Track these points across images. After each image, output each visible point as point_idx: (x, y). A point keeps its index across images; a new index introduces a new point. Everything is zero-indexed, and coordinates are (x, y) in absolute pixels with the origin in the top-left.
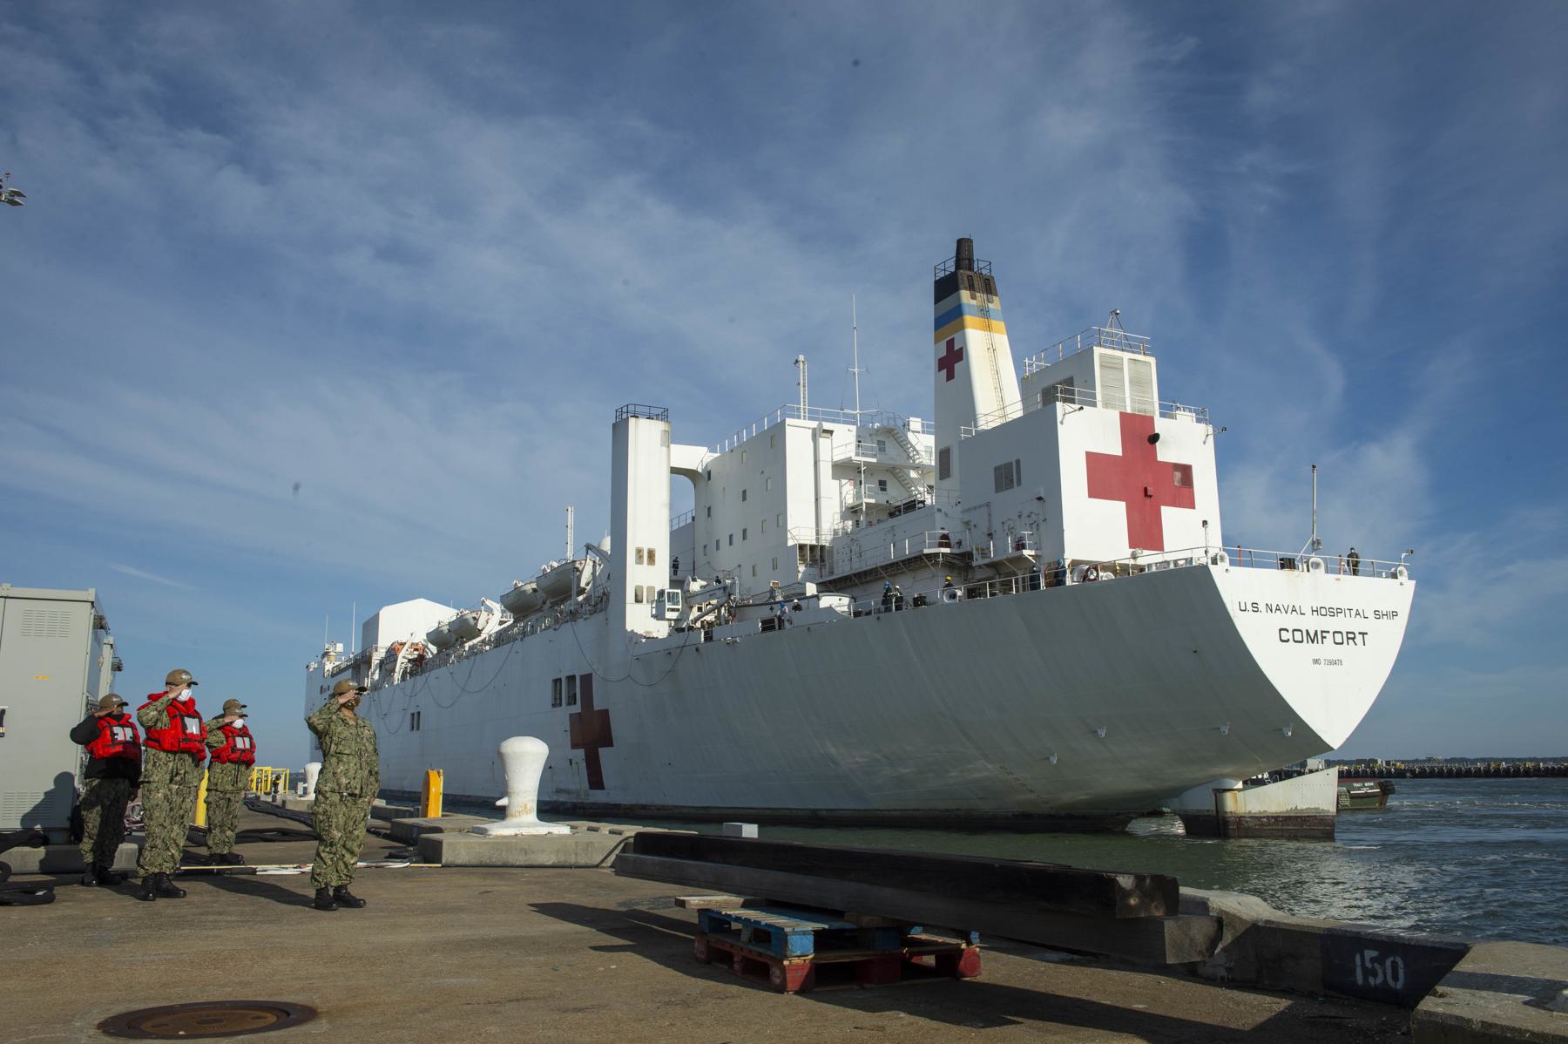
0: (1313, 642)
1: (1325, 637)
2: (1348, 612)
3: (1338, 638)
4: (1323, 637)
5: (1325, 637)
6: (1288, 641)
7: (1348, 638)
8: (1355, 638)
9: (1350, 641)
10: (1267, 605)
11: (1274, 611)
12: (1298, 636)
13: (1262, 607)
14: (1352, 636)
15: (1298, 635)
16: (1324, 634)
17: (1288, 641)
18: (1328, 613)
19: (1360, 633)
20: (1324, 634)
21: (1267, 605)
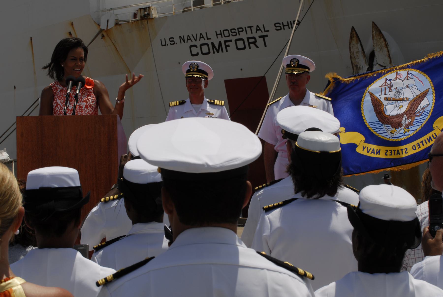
0: (218, 51)
1: (228, 46)
3: (240, 44)
4: (227, 46)
5: (228, 46)
6: (197, 54)
7: (249, 43)
8: (256, 41)
9: (252, 46)
10: (180, 37)
11: (186, 40)
13: (177, 40)
14: (253, 40)
16: (227, 44)
18: (231, 34)
19: (260, 37)
20: (227, 44)
21: (180, 37)
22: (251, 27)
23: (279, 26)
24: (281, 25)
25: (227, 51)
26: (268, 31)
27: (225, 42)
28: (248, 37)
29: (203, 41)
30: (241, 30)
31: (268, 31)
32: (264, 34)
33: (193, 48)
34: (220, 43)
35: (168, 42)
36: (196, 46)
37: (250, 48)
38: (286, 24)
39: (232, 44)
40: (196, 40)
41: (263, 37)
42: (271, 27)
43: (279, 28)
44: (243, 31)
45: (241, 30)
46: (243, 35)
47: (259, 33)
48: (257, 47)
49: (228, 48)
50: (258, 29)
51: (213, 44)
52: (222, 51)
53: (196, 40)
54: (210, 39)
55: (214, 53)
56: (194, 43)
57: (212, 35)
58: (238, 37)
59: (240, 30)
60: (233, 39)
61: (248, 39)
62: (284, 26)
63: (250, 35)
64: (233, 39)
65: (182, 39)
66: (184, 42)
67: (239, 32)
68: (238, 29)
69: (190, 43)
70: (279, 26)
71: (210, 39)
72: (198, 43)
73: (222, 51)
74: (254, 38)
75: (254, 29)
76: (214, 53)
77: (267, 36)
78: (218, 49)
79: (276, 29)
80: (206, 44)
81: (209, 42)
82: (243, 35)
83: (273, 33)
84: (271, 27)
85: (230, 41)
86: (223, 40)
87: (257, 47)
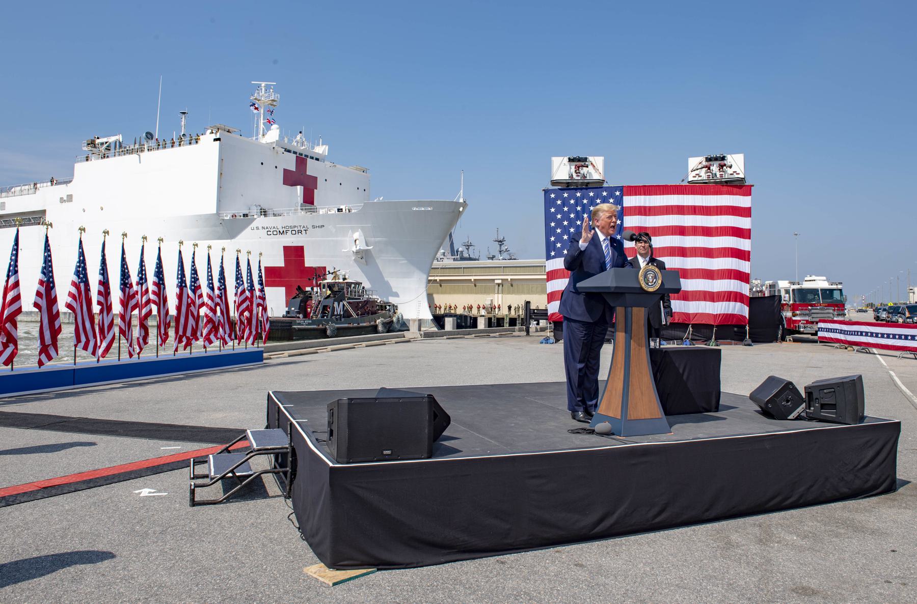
3: (294, 232)
12: (275, 233)
13: (260, 228)
23: (314, 227)
29: (274, 230)
32: (306, 229)
34: (283, 231)
35: (255, 228)
42: (310, 227)
47: (304, 229)
50: (304, 227)
51: (279, 231)
58: (293, 229)
59: (295, 227)
65: (263, 228)
69: (267, 230)
70: (314, 227)
72: (272, 230)
75: (302, 227)
81: (278, 231)
82: (296, 229)
84: (310, 227)
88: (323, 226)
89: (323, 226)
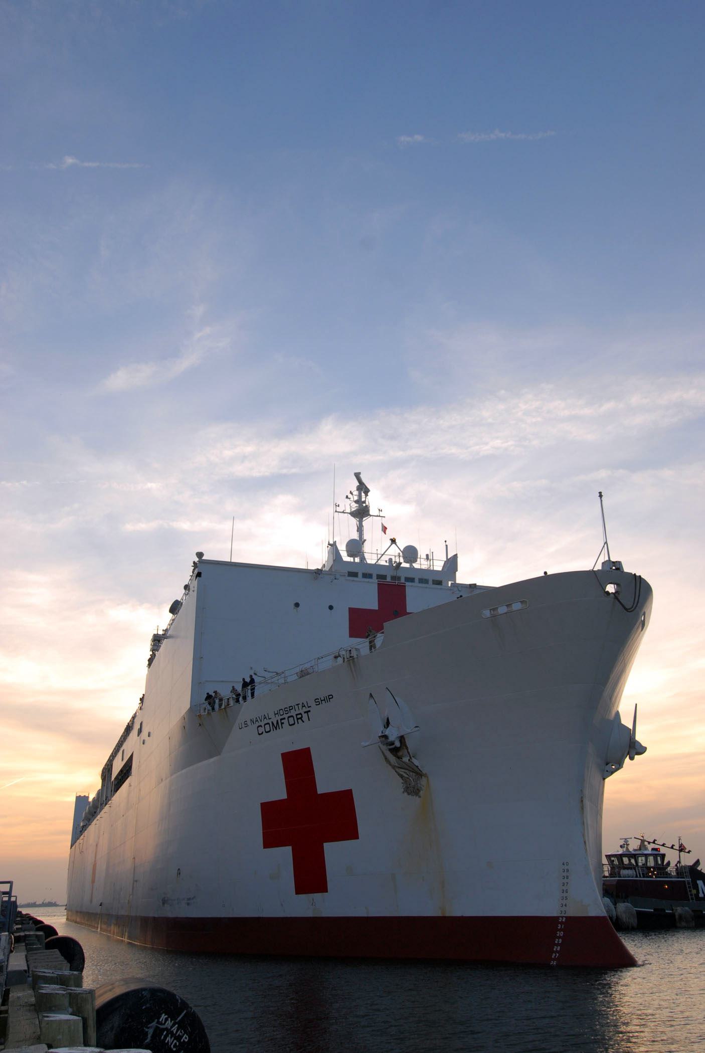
0: (276, 729)
1: (283, 723)
2: (296, 707)
3: (291, 720)
5: (283, 723)
6: (262, 733)
7: (298, 719)
8: (302, 717)
9: (300, 720)
13: (249, 723)
14: (299, 716)
15: (267, 726)
17: (262, 733)
19: (305, 712)
20: (282, 721)
22: (298, 705)
23: (318, 702)
24: (320, 701)
25: (282, 728)
26: (310, 707)
27: (281, 720)
28: (297, 713)
29: (266, 721)
30: (291, 708)
31: (310, 707)
32: (308, 709)
33: (259, 728)
35: (243, 726)
36: (261, 726)
37: (298, 723)
38: (323, 699)
39: (285, 721)
40: (261, 721)
41: (307, 712)
42: (312, 703)
43: (318, 703)
44: (292, 709)
45: (291, 708)
46: (293, 713)
48: (303, 722)
49: (283, 725)
52: (279, 728)
53: (261, 721)
54: (270, 719)
55: (273, 730)
56: (260, 724)
57: (272, 715)
59: (291, 708)
60: (286, 716)
61: (297, 715)
62: (321, 701)
63: (298, 712)
64: (286, 716)
66: (253, 722)
67: (290, 710)
68: (289, 707)
70: (318, 702)
71: (270, 719)
72: (262, 724)
73: (279, 728)
74: (300, 714)
75: (300, 706)
76: (273, 730)
77: (309, 711)
78: (276, 726)
79: (317, 705)
80: (268, 724)
82: (293, 713)
83: (314, 709)
84: (312, 703)
85: (284, 719)
86: (279, 718)
87: (303, 722)
88: (330, 697)
89: (330, 697)
